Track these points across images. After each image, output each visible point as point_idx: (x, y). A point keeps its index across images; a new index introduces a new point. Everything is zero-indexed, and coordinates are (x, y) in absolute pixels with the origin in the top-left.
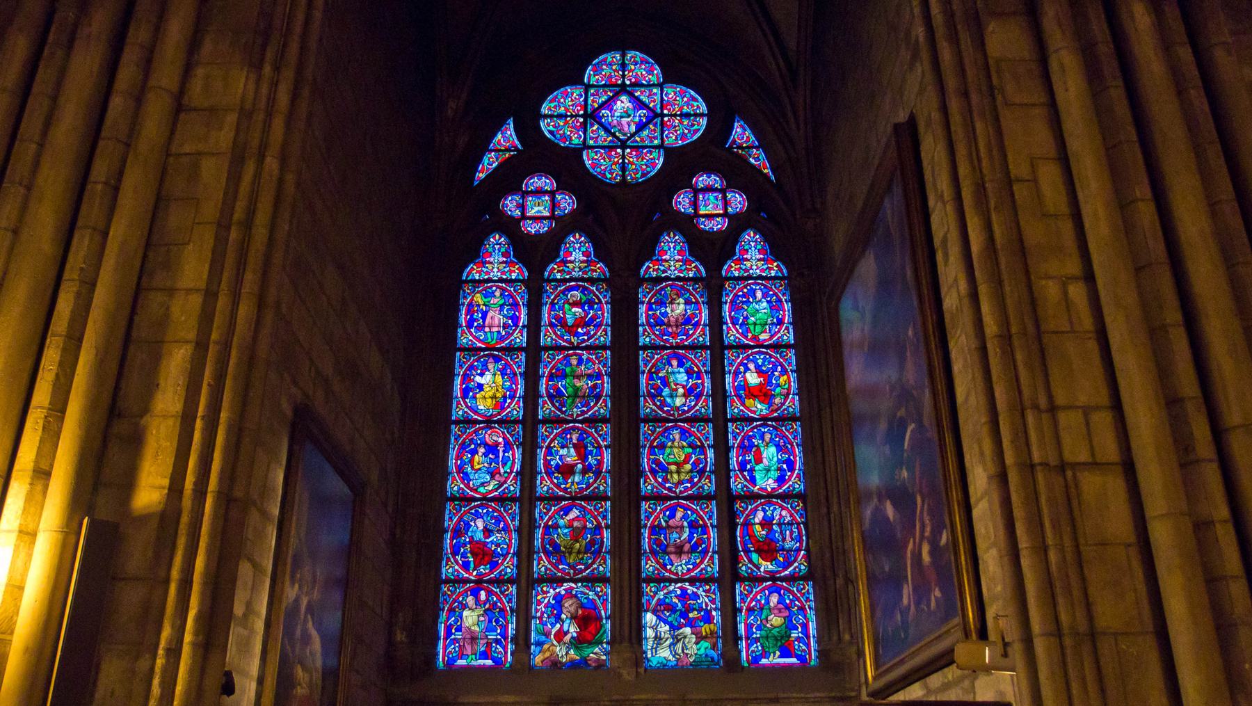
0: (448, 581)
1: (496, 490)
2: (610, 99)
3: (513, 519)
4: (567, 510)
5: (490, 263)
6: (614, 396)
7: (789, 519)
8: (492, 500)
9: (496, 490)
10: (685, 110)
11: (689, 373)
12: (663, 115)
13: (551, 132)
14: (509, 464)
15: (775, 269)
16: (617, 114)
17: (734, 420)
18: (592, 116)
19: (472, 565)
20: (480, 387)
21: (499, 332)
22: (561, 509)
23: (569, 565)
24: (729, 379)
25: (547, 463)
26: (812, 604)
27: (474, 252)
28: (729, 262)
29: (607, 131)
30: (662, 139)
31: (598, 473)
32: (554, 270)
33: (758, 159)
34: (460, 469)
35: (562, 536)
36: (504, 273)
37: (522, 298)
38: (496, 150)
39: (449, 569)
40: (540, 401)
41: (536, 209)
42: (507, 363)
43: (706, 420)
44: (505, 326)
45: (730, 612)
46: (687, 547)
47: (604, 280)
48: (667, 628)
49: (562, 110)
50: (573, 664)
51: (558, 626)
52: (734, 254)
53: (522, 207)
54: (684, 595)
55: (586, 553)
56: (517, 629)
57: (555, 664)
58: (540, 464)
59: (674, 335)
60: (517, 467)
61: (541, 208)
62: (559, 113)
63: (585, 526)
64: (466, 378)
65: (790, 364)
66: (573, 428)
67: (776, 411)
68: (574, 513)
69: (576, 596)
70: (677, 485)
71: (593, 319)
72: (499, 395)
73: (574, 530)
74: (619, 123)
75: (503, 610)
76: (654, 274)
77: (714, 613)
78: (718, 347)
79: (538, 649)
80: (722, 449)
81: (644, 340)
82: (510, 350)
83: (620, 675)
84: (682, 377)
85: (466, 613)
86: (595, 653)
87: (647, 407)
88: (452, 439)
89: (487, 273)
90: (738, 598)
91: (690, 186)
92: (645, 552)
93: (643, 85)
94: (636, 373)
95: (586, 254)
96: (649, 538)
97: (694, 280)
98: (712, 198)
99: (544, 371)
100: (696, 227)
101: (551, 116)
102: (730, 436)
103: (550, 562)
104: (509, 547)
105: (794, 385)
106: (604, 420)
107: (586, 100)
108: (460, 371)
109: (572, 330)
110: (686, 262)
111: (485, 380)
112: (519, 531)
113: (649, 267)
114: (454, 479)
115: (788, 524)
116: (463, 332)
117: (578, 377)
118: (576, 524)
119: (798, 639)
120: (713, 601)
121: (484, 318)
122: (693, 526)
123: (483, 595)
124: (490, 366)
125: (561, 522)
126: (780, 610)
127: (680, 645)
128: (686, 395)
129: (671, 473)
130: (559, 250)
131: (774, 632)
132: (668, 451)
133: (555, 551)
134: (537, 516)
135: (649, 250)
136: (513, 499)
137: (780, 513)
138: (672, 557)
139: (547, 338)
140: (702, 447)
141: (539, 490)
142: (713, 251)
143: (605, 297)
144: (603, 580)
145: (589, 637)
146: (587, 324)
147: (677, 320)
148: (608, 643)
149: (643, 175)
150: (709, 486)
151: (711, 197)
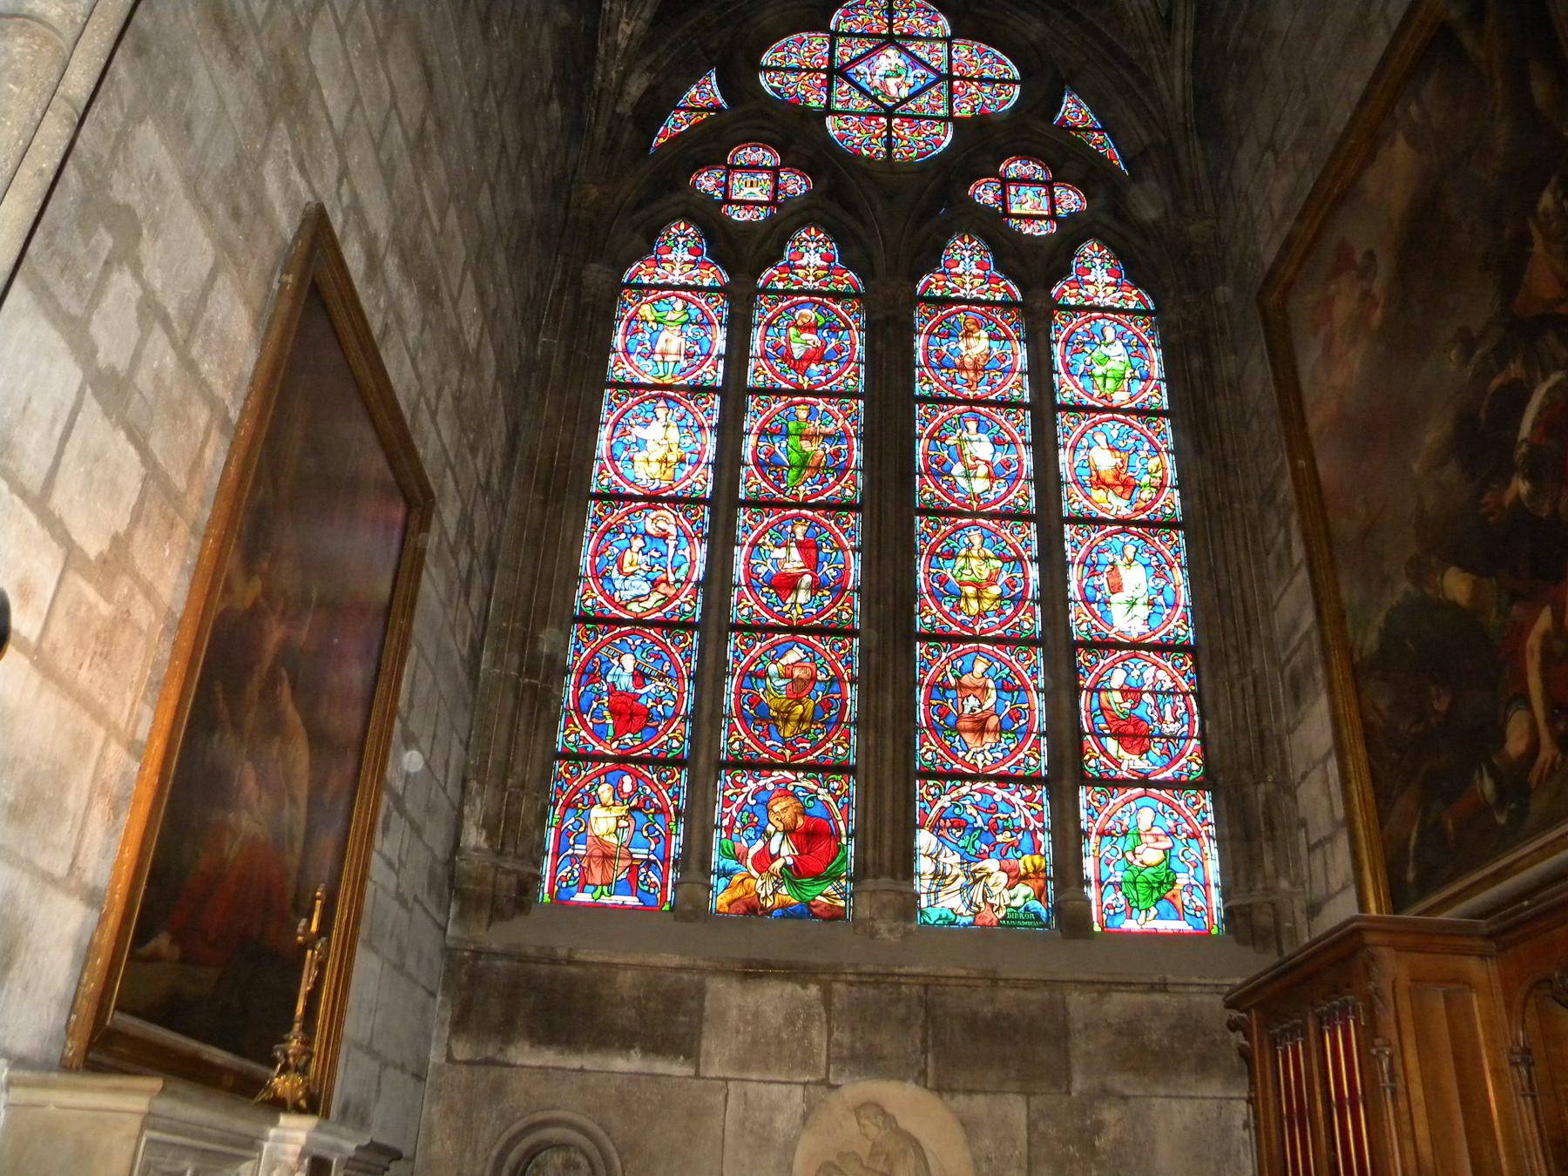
0: (565, 756)
1: (660, 608)
2: (869, 53)
3: (688, 659)
5: (667, 261)
6: (867, 469)
7: (1168, 685)
8: (654, 624)
9: (660, 608)
10: (986, 74)
11: (996, 442)
12: (951, 78)
14: (685, 568)
16: (879, 72)
17: (1073, 520)
18: (837, 72)
19: (611, 732)
20: (641, 444)
22: (773, 646)
24: (1064, 457)
25: (750, 573)
26: (1212, 830)
28: (1060, 285)
29: (862, 91)
30: (951, 108)
31: (839, 590)
32: (771, 276)
33: (1102, 143)
34: (600, 575)
35: (774, 690)
37: (720, 314)
38: (686, 109)
39: (566, 738)
40: (743, 471)
41: (748, 190)
43: (1025, 518)
44: (688, 355)
45: (1068, 838)
46: (993, 722)
47: (857, 295)
48: (957, 858)
49: (794, 63)
50: (787, 912)
51: (760, 844)
52: (1069, 273)
57: (752, 909)
58: (739, 571)
60: (699, 572)
61: (756, 190)
62: (790, 67)
63: (814, 679)
65: (1164, 441)
67: (1144, 510)
68: (794, 656)
69: (794, 795)
74: (883, 84)
75: (662, 811)
77: (1040, 836)
79: (723, 881)
80: (1052, 561)
81: (920, 388)
82: (697, 389)
83: (873, 934)
84: (982, 448)
85: (596, 811)
86: (824, 894)
87: (926, 491)
90: (1083, 814)
93: (919, 38)
94: (910, 439)
95: (827, 258)
97: (1005, 305)
98: (1030, 193)
99: (751, 423)
101: (777, 69)
102: (1067, 546)
103: (749, 734)
104: (678, 703)
105: (1172, 475)
106: (851, 507)
107: (832, 51)
110: (990, 279)
111: (654, 432)
112: (696, 678)
113: (929, 283)
114: (588, 588)
115: (1168, 692)
116: (618, 360)
117: (809, 437)
118: (797, 673)
120: (1040, 820)
121: (654, 342)
122: (1004, 687)
124: (661, 413)
125: (773, 669)
127: (979, 889)
128: (991, 476)
129: (966, 597)
130: (782, 248)
131: (1148, 873)
132: (961, 562)
134: (730, 656)
135: (930, 256)
136: (689, 626)
137: (1154, 673)
138: (968, 737)
140: (1020, 558)
141: (734, 612)
142: (1035, 270)
143: (857, 320)
144: (843, 769)
145: (812, 863)
146: (819, 361)
147: (976, 361)
148: (848, 879)
149: (920, 155)
150: (1031, 622)
151: (1029, 193)
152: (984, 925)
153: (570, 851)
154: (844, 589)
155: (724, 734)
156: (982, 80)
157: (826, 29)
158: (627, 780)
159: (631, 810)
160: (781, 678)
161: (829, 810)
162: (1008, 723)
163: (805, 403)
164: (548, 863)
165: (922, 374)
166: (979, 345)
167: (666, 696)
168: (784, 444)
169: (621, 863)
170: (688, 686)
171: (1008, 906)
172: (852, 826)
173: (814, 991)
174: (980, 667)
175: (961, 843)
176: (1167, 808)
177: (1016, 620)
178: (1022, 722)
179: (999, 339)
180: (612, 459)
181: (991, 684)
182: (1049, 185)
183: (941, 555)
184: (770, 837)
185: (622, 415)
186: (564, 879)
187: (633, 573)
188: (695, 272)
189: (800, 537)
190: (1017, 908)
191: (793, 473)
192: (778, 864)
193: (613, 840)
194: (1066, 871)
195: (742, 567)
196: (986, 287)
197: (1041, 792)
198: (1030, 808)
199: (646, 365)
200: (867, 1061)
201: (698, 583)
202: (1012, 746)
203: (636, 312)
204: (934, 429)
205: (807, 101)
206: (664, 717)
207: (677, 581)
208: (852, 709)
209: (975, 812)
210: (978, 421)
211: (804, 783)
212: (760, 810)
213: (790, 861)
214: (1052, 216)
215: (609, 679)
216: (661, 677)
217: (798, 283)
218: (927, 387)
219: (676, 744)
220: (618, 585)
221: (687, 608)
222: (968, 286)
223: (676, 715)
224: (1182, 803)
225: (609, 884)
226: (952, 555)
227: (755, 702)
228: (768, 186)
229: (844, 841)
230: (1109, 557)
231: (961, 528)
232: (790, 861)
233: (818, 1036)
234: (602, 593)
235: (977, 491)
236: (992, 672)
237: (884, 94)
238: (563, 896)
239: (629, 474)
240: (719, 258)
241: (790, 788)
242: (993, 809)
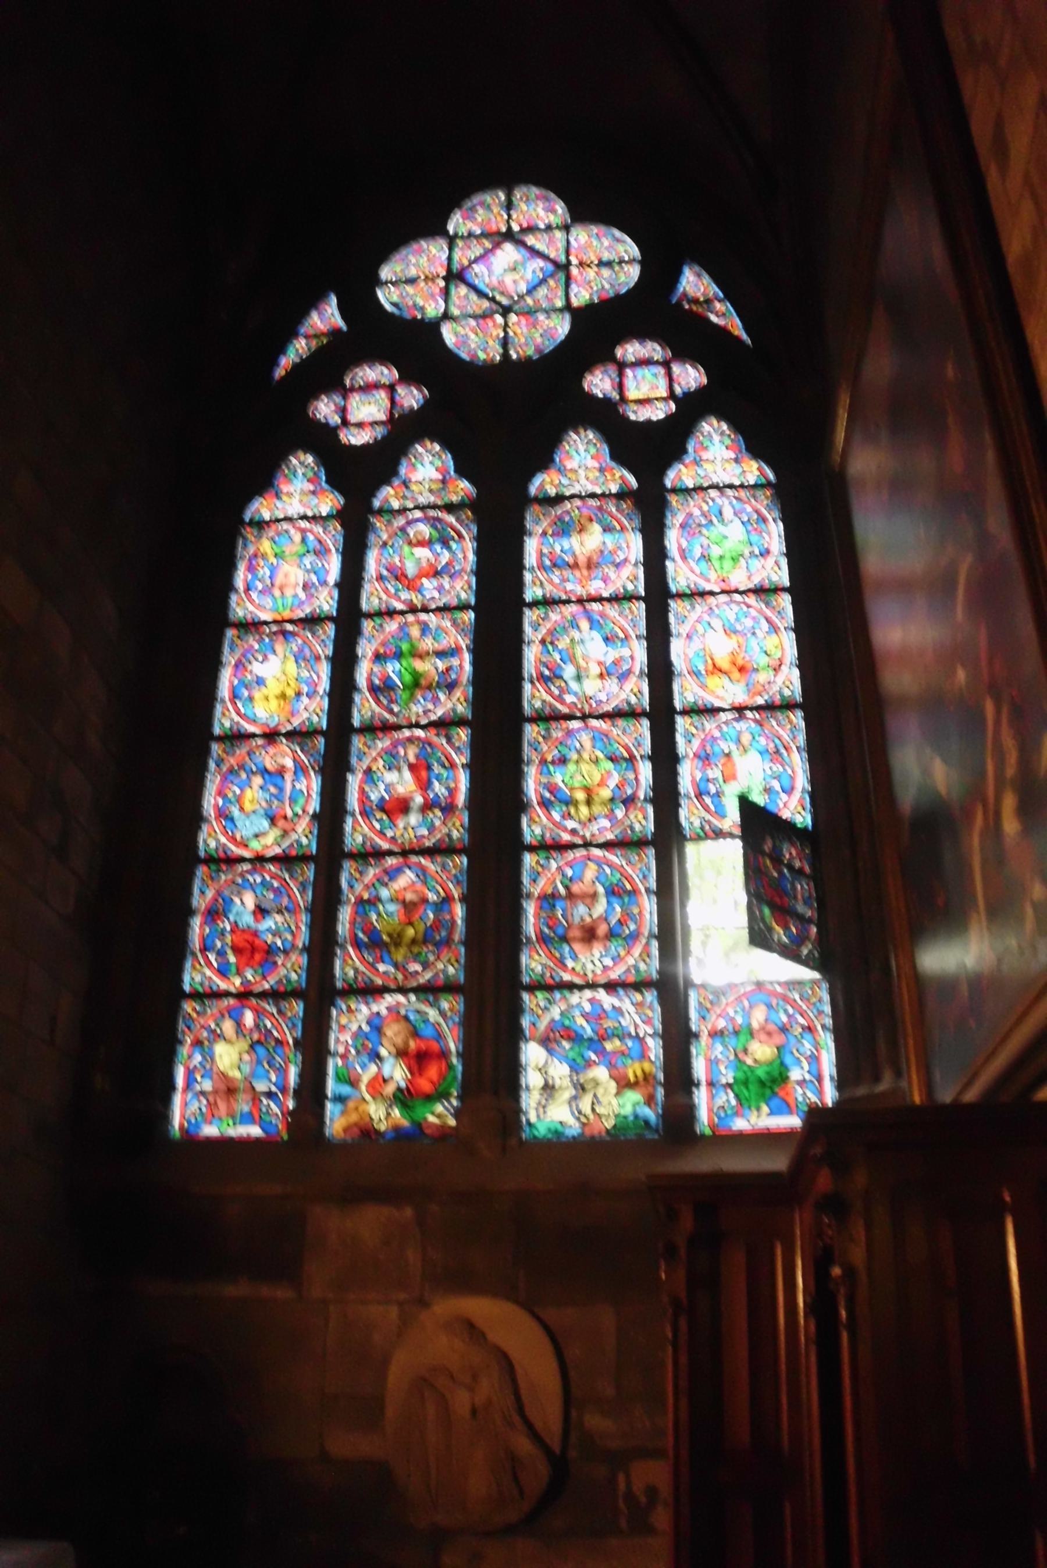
4: (392, 874)
8: (275, 859)
10: (606, 256)
13: (395, 305)
14: (301, 801)
15: (753, 471)
18: (455, 276)
19: (233, 969)
20: (260, 682)
21: (296, 596)
23: (396, 966)
26: (829, 1022)
27: (264, 480)
32: (388, 495)
33: (724, 316)
34: (223, 814)
39: (192, 977)
46: (602, 930)
51: (373, 1069)
53: (343, 411)
54: (597, 1016)
55: (425, 941)
60: (314, 805)
62: (410, 280)
64: (240, 666)
66: (410, 740)
68: (408, 877)
69: (406, 1018)
70: (584, 824)
72: (290, 693)
77: (650, 1041)
78: (658, 596)
80: (665, 758)
82: (312, 621)
87: (534, 697)
88: (212, 765)
91: (613, 359)
92: (529, 939)
96: (537, 915)
97: (620, 496)
99: (365, 648)
100: (625, 419)
106: (461, 722)
108: (229, 658)
109: (412, 585)
119: (802, 1083)
120: (648, 1021)
123: (249, 1018)
125: (384, 893)
126: (769, 1034)
131: (761, 1072)
132: (571, 767)
133: (374, 944)
136: (305, 858)
138: (577, 947)
139: (371, 597)
141: (348, 841)
142: (649, 451)
145: (425, 1085)
146: (436, 574)
155: (338, 963)
156: (601, 264)
157: (444, 233)
159: (252, 1046)
162: (618, 930)
164: (177, 1100)
166: (591, 540)
167: (287, 929)
173: (409, 1212)
176: (781, 1003)
182: (666, 364)
183: (553, 762)
189: (412, 759)
192: (390, 1089)
193: (236, 1074)
194: (678, 1076)
195: (356, 795)
197: (650, 996)
199: (268, 602)
200: (462, 1280)
205: (422, 309)
210: (590, 619)
212: (374, 1037)
213: (403, 1084)
214: (672, 395)
216: (280, 912)
220: (239, 824)
224: (797, 997)
225: (233, 1117)
226: (563, 761)
228: (386, 403)
230: (724, 746)
232: (403, 1084)
233: (413, 1256)
235: (589, 692)
237: (502, 293)
239: (249, 714)
240: (336, 482)
241: (403, 1012)
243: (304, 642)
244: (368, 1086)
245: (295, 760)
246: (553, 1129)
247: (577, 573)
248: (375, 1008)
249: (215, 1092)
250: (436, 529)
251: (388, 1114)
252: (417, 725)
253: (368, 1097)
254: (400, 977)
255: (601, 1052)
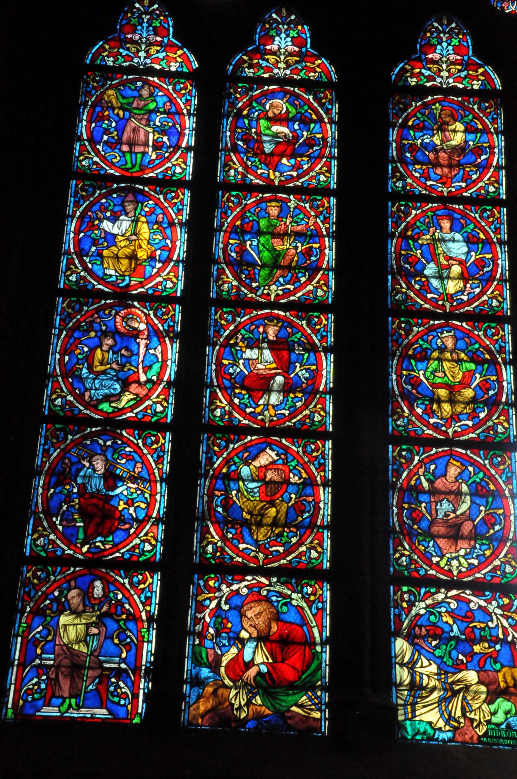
0: (35, 560)
1: (132, 408)
3: (159, 460)
5: (132, 41)
11: (471, 241)
14: (156, 367)
19: (81, 536)
20: (111, 239)
21: (144, 154)
22: (245, 448)
31: (311, 391)
34: (69, 372)
36: (157, 60)
37: (188, 102)
42: (158, 203)
44: (157, 146)
46: (467, 528)
48: (434, 668)
51: (234, 651)
56: (156, 655)
59: (445, 181)
60: (171, 372)
63: (287, 482)
64: (88, 223)
69: (267, 599)
71: (310, 143)
72: (142, 254)
73: (267, 484)
75: (134, 617)
76: (413, 81)
84: (458, 248)
89: (128, 58)
95: (297, 41)
96: (401, 509)
97: (483, 95)
104: (150, 505)
106: (323, 308)
109: (271, 161)
110: (468, 65)
113: (403, 70)
114: (56, 386)
116: (83, 148)
117: (281, 236)
121: (121, 130)
123: (98, 588)
124: (129, 207)
125: (245, 471)
128: (464, 277)
129: (439, 401)
132: (434, 364)
134: (203, 457)
136: (161, 427)
138: (441, 542)
140: (493, 362)
143: (328, 112)
144: (316, 574)
145: (287, 672)
152: (464, 743)
153: (38, 661)
154: (318, 392)
158: (98, 585)
160: (253, 480)
161: (303, 617)
162: (483, 529)
163: (277, 200)
165: (395, 169)
168: (255, 243)
169: (91, 673)
170: (161, 488)
171: (489, 722)
172: (327, 633)
174: (453, 471)
175: (438, 653)
177: (490, 423)
178: (497, 528)
179: (476, 131)
180: (81, 253)
181: (465, 488)
184: (243, 642)
185: (88, 208)
186: (29, 692)
187: (104, 372)
188: (161, 55)
190: (498, 725)
191: (264, 273)
192: (252, 672)
196: (463, 74)
198: (507, 618)
201: (169, 383)
202: (488, 553)
203: (100, 98)
204: (406, 229)
206: (136, 520)
207: (149, 381)
208: (326, 511)
209: (451, 622)
211: (277, 588)
212: (233, 616)
215: (79, 481)
216: (134, 479)
217: (268, 69)
218: (400, 184)
219: (148, 547)
221: (159, 408)
222: (445, 74)
223: (148, 517)
225: (77, 696)
226: (424, 356)
227: (227, 503)
229: (318, 649)
231: (433, 329)
232: (264, 669)
234: (72, 392)
236: (465, 476)
238: (29, 711)
242: (468, 617)
243: (156, 204)
244: (227, 667)
245: (147, 324)
246: (422, 730)
247: (439, 171)
248: (235, 587)
249: (57, 667)
250: (293, 104)
251: (249, 703)
252: (275, 305)
253: (227, 682)
254: (261, 556)
255: (470, 655)
